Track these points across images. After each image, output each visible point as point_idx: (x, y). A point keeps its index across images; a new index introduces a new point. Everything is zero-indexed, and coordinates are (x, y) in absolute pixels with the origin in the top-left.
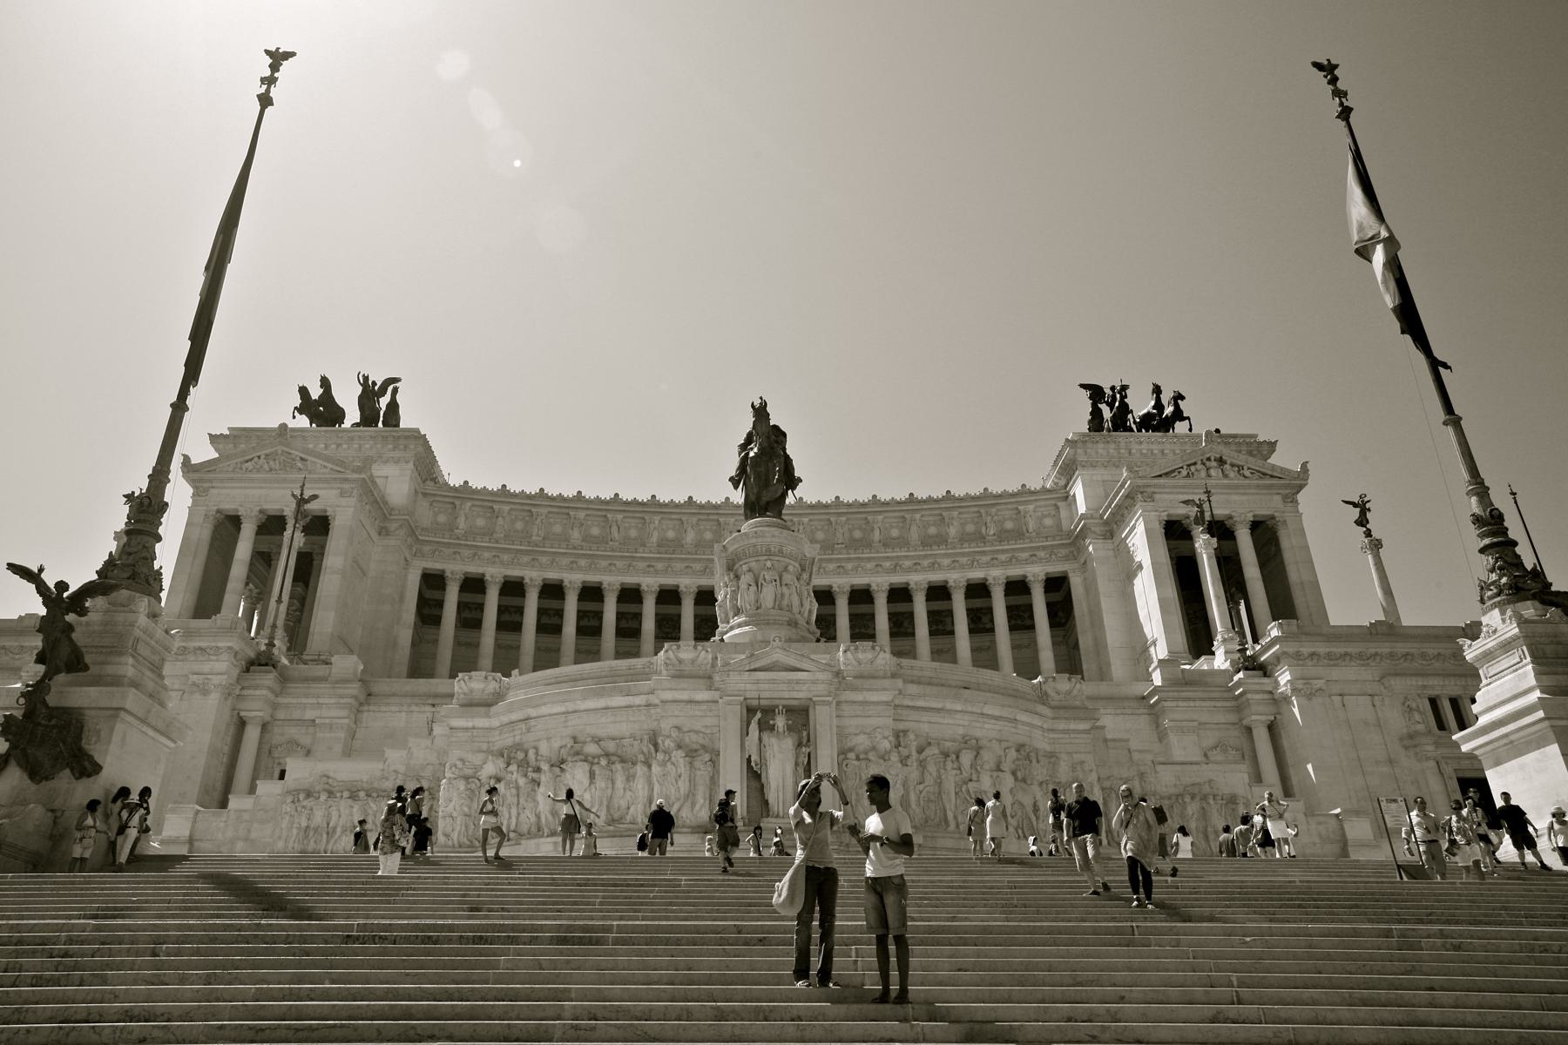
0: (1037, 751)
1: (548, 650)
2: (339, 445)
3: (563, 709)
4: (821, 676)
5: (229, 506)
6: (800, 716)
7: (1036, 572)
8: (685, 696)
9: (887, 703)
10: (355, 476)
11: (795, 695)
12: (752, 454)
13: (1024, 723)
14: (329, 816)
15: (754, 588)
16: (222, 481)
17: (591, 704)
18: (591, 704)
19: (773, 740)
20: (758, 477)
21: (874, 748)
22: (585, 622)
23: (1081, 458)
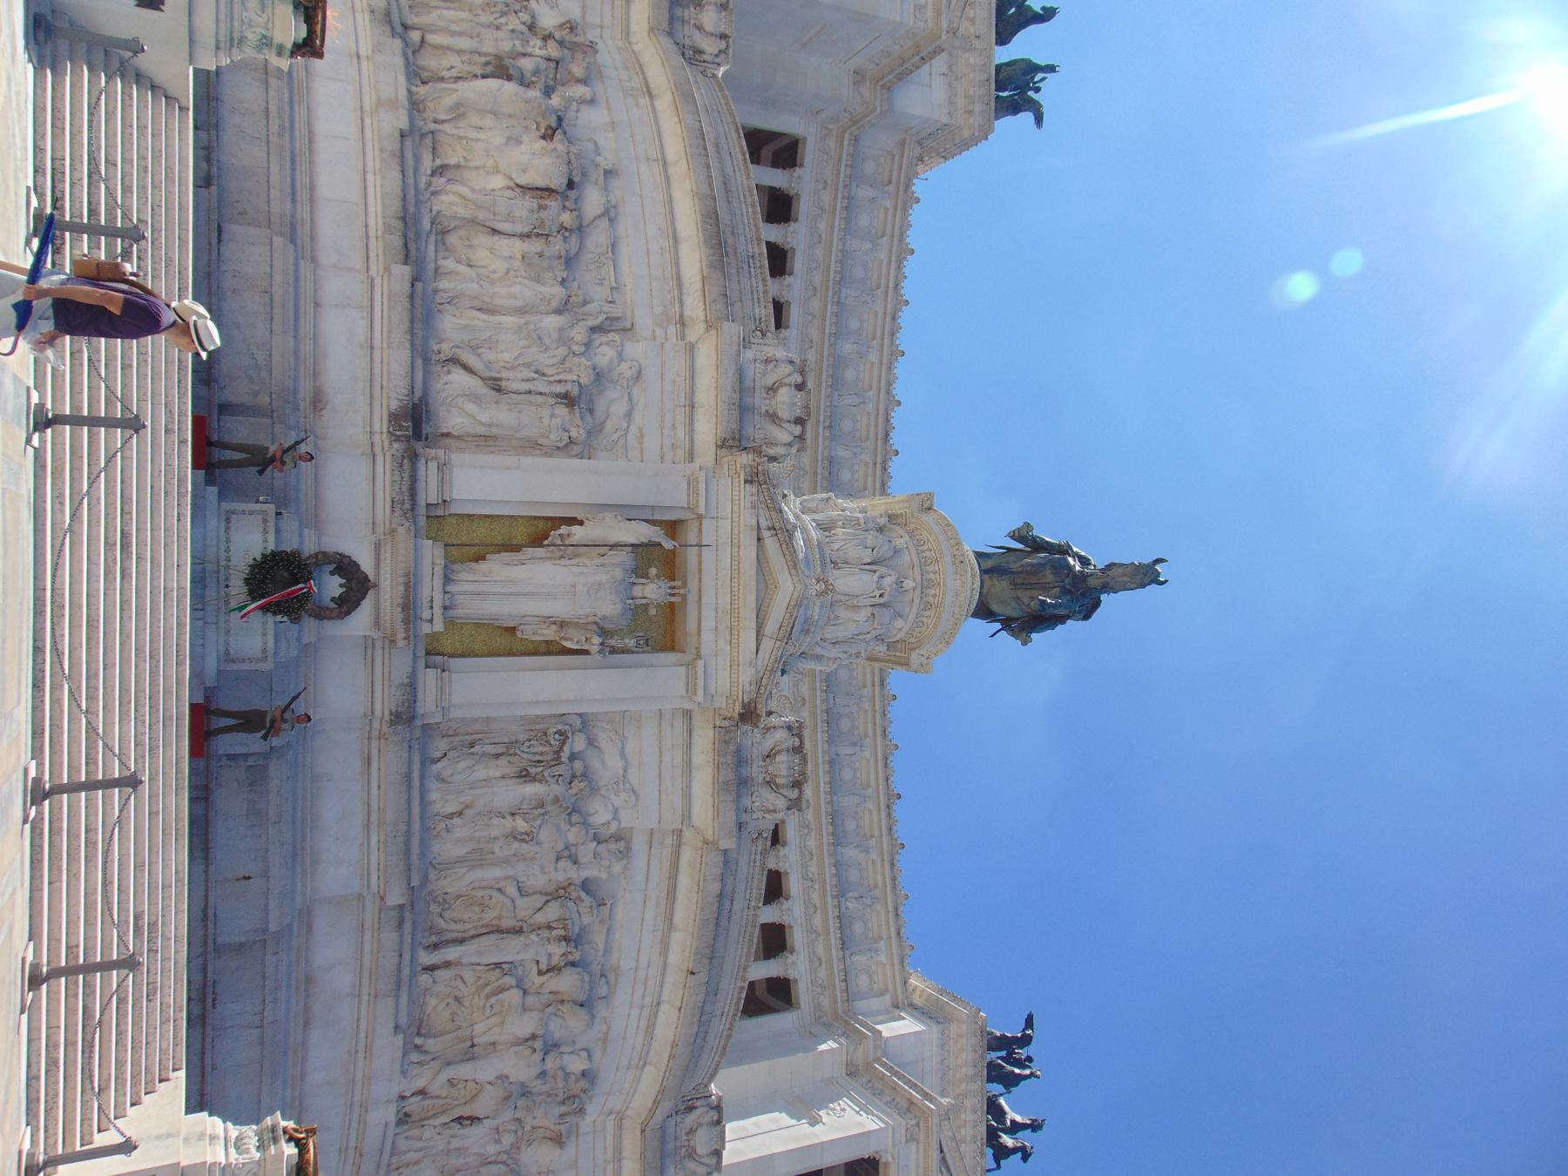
3: (671, 157)
4: (746, 676)
9: (687, 816)
10: (944, 24)
11: (708, 624)
12: (1070, 560)
13: (637, 1081)
19: (619, 573)
20: (1037, 569)
21: (594, 789)
23: (954, 1029)
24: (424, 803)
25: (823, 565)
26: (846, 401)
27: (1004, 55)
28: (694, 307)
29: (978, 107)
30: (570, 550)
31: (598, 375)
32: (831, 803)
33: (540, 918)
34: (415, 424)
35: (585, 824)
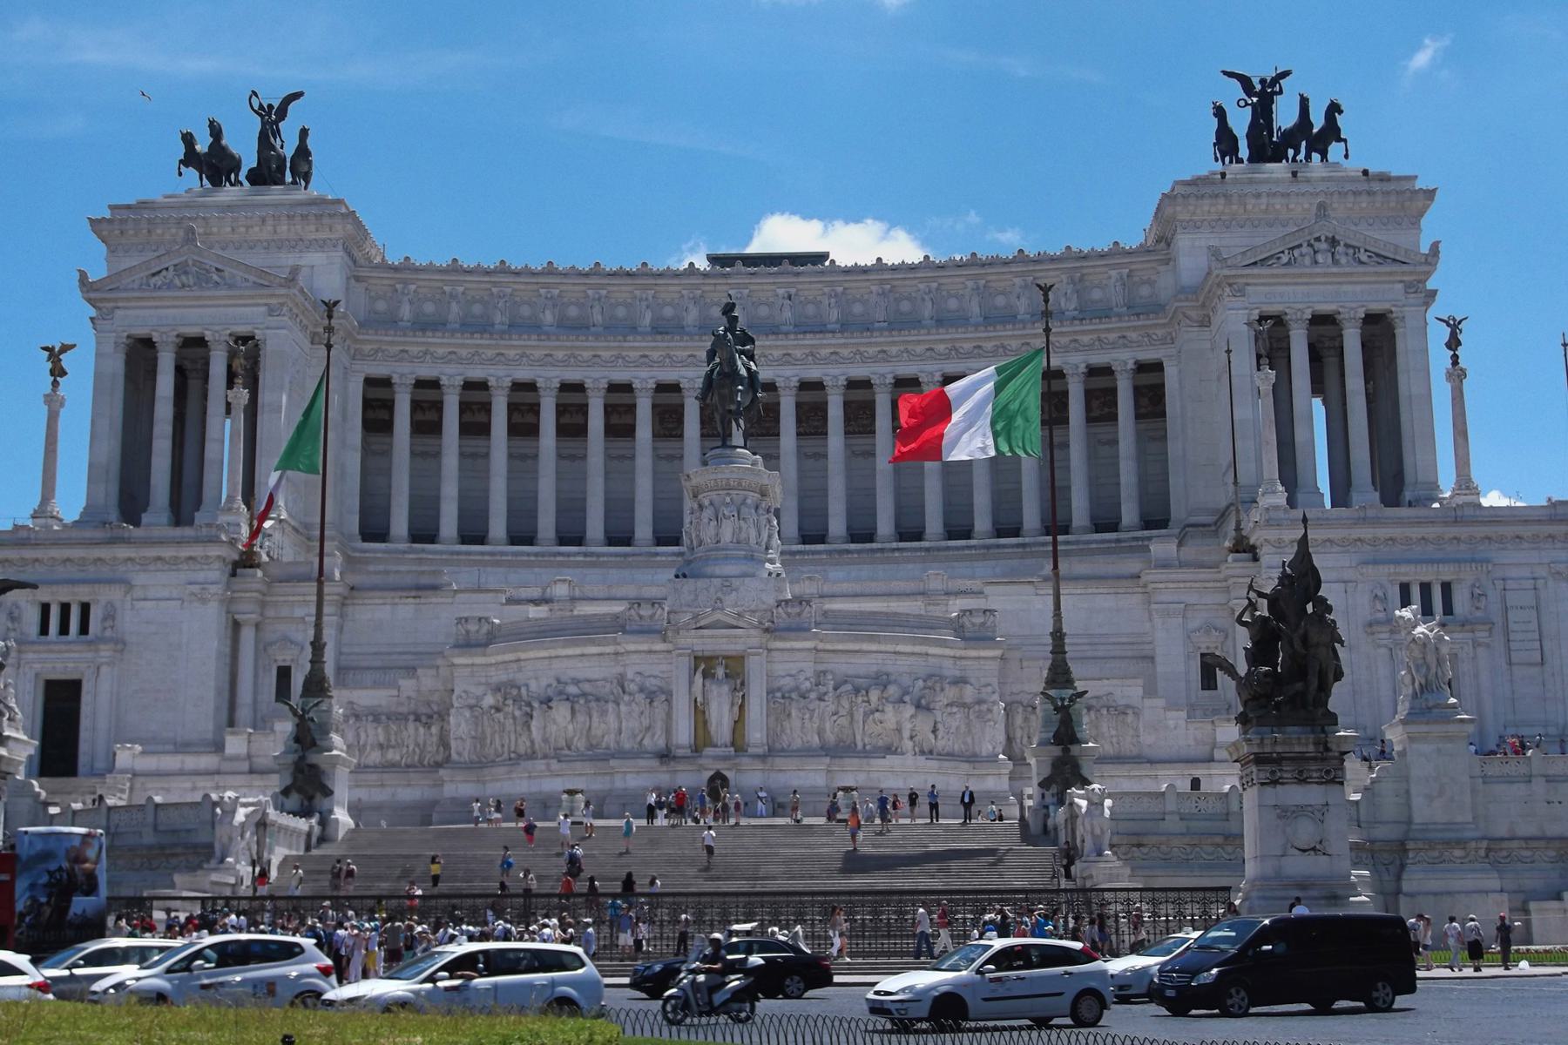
0: (942, 678)
1: (523, 457)
2: (247, 228)
4: (752, 632)
5: (141, 331)
6: (733, 670)
7: (1123, 359)
8: (645, 647)
10: (283, 291)
11: (732, 647)
14: (358, 735)
15: (714, 523)
16: (128, 299)
17: (570, 651)
18: (570, 651)
21: (797, 688)
22: (566, 420)
24: (798, 750)
25: (717, 549)
26: (598, 318)
27: (249, 161)
28: (609, 649)
29: (326, 220)
30: (706, 703)
31: (641, 690)
32: (976, 326)
33: (847, 706)
34: (665, 756)
35: (810, 691)
